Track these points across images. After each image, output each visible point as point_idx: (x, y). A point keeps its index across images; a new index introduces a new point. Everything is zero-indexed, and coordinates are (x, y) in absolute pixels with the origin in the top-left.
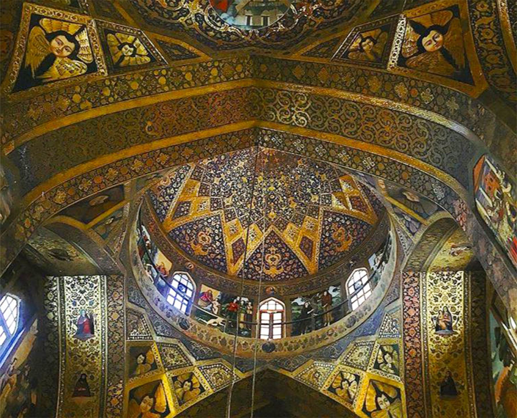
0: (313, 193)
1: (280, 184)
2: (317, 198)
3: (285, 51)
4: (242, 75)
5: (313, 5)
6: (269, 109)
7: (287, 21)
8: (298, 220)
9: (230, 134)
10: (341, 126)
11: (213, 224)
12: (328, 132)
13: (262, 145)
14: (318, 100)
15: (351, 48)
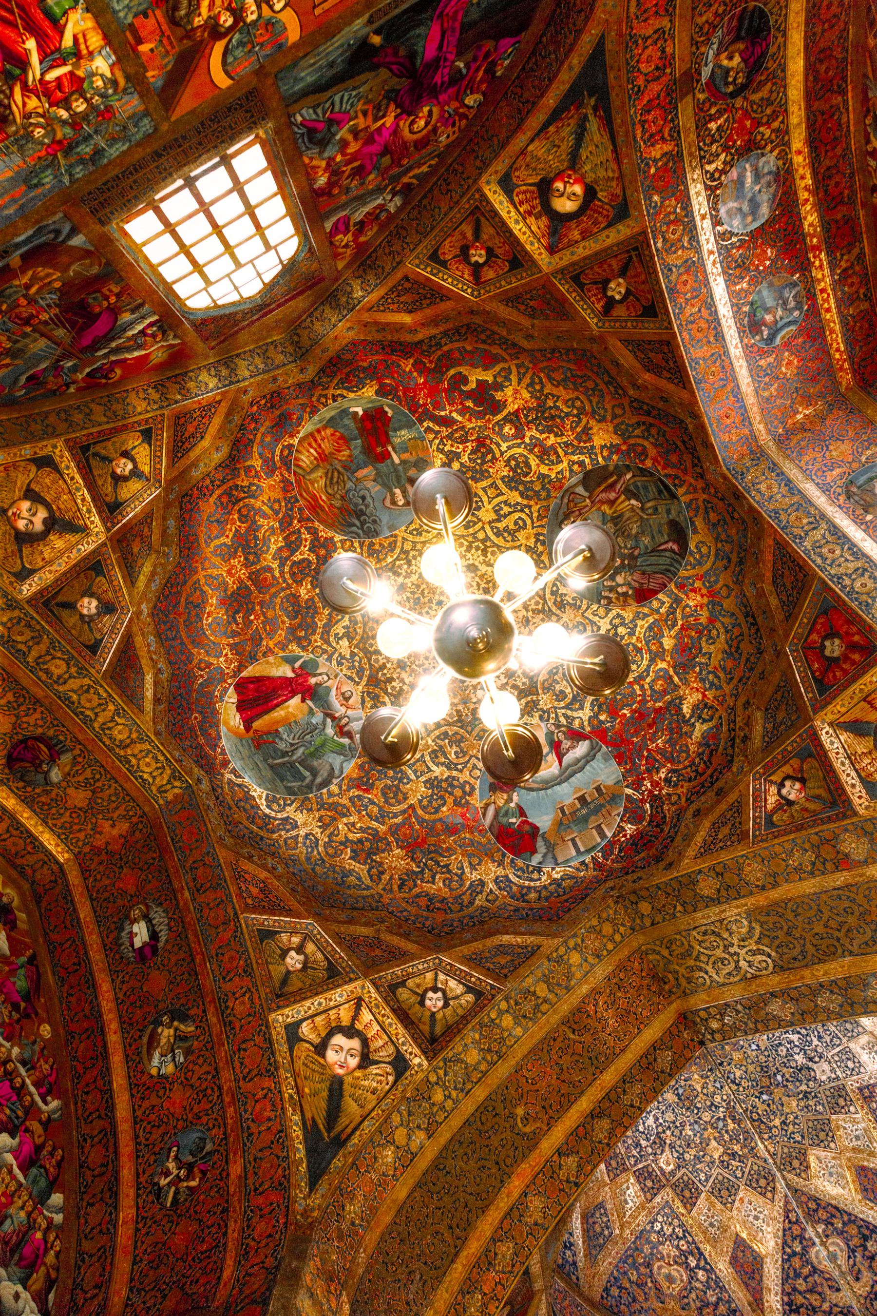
0: (811, 1059)
1: (738, 1073)
2: (826, 1066)
3: (662, 865)
4: (617, 938)
5: (658, 772)
6: (691, 969)
7: (633, 813)
8: (822, 1133)
9: (652, 1051)
10: (838, 940)
11: (668, 1231)
12: (821, 961)
13: (713, 1040)
14: (768, 914)
15: (769, 807)
